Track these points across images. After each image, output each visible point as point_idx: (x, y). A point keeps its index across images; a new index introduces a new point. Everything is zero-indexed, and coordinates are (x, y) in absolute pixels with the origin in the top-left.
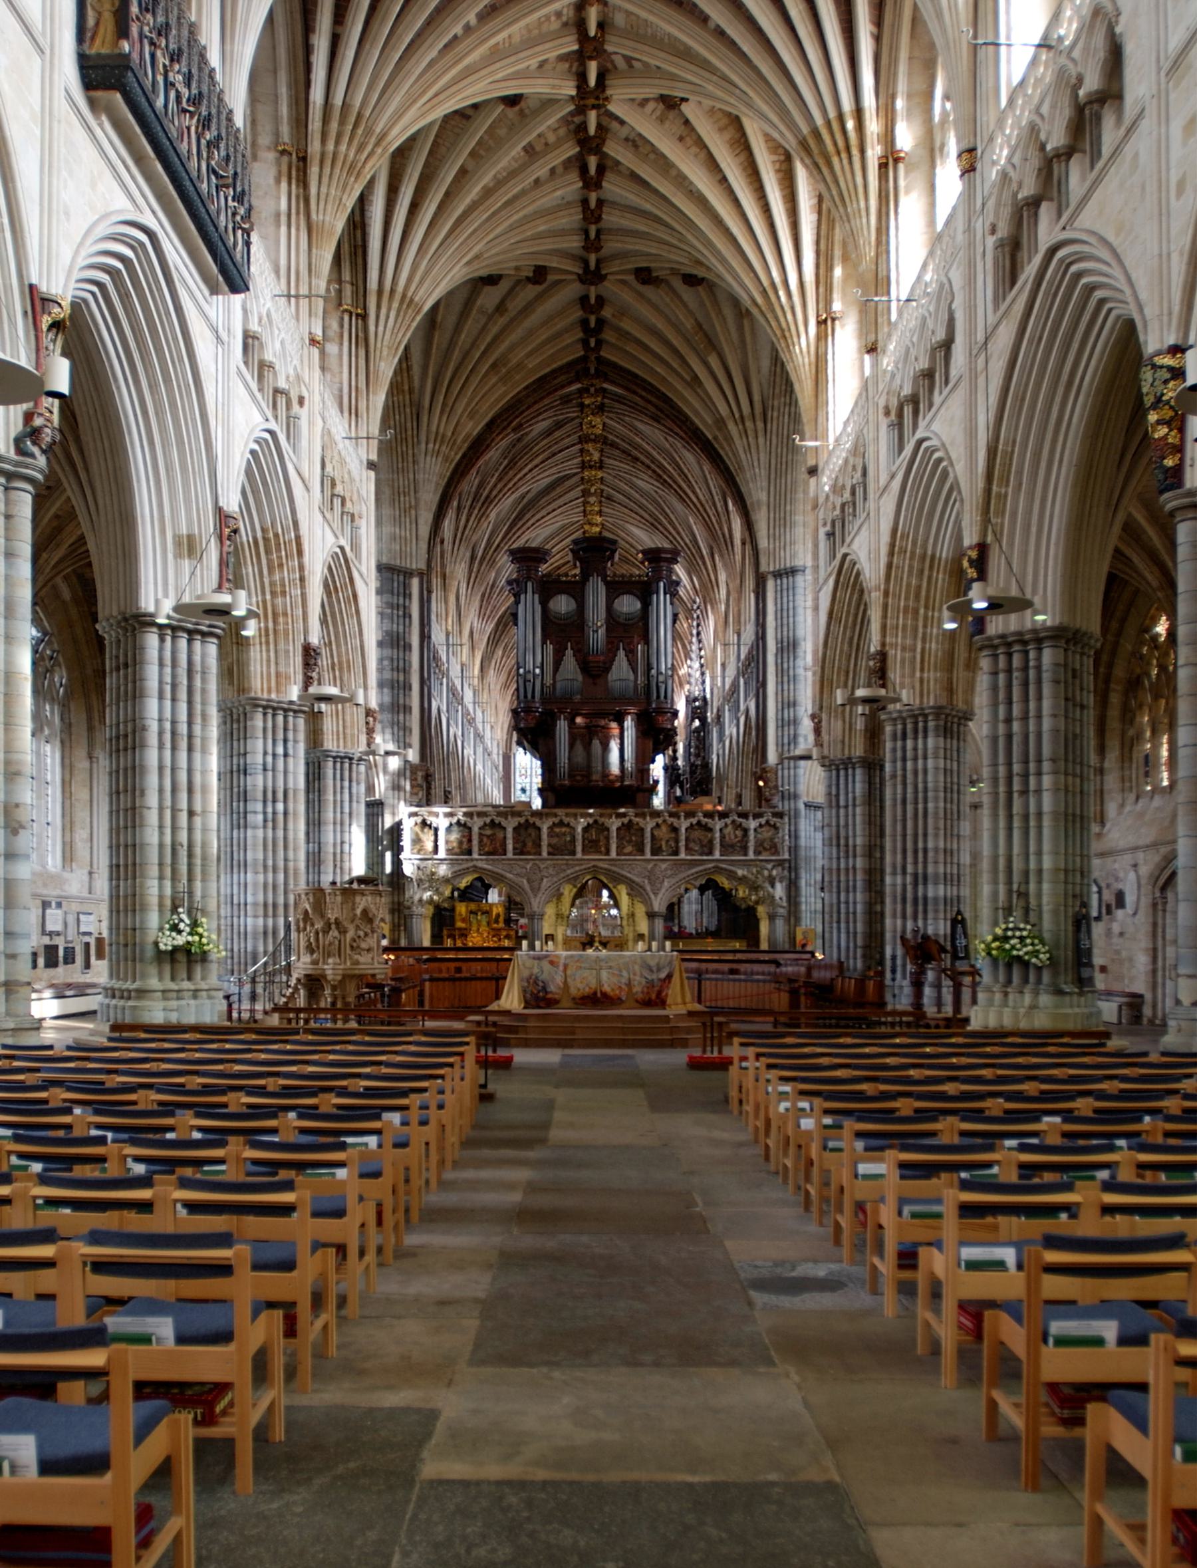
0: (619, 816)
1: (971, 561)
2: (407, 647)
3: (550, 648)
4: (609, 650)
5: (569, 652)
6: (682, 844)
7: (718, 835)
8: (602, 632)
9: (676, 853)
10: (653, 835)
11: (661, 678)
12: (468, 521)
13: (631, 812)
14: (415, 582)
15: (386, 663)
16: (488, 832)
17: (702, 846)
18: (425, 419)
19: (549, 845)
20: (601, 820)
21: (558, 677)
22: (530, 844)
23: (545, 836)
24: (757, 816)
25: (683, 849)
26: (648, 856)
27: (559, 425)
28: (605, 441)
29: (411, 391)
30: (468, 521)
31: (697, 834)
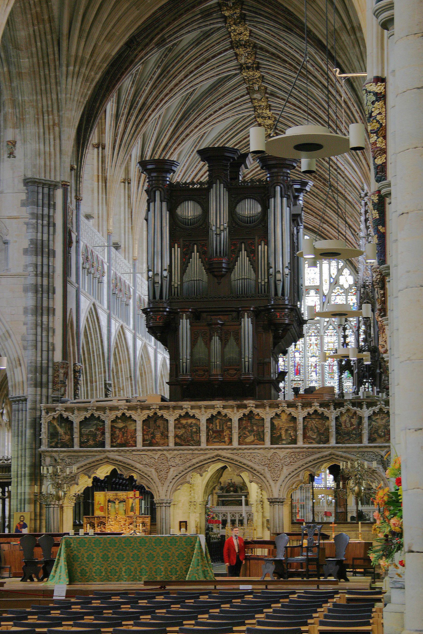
0: (239, 407)
1: (374, 204)
2: (51, 253)
3: (177, 251)
4: (233, 252)
5: (196, 255)
6: (300, 432)
7: (333, 423)
8: (224, 235)
9: (294, 441)
10: (272, 424)
11: (279, 276)
12: (126, 127)
13: (251, 403)
14: (59, 193)
15: (31, 269)
16: (120, 425)
17: (320, 434)
18: (64, 44)
19: (176, 436)
20: (224, 412)
21: (185, 279)
22: (158, 435)
23: (171, 427)
24: (370, 405)
25: (300, 438)
26: (268, 444)
27: (207, 35)
28: (255, 46)
29: (51, 20)
30: (126, 127)
31: (314, 423)
